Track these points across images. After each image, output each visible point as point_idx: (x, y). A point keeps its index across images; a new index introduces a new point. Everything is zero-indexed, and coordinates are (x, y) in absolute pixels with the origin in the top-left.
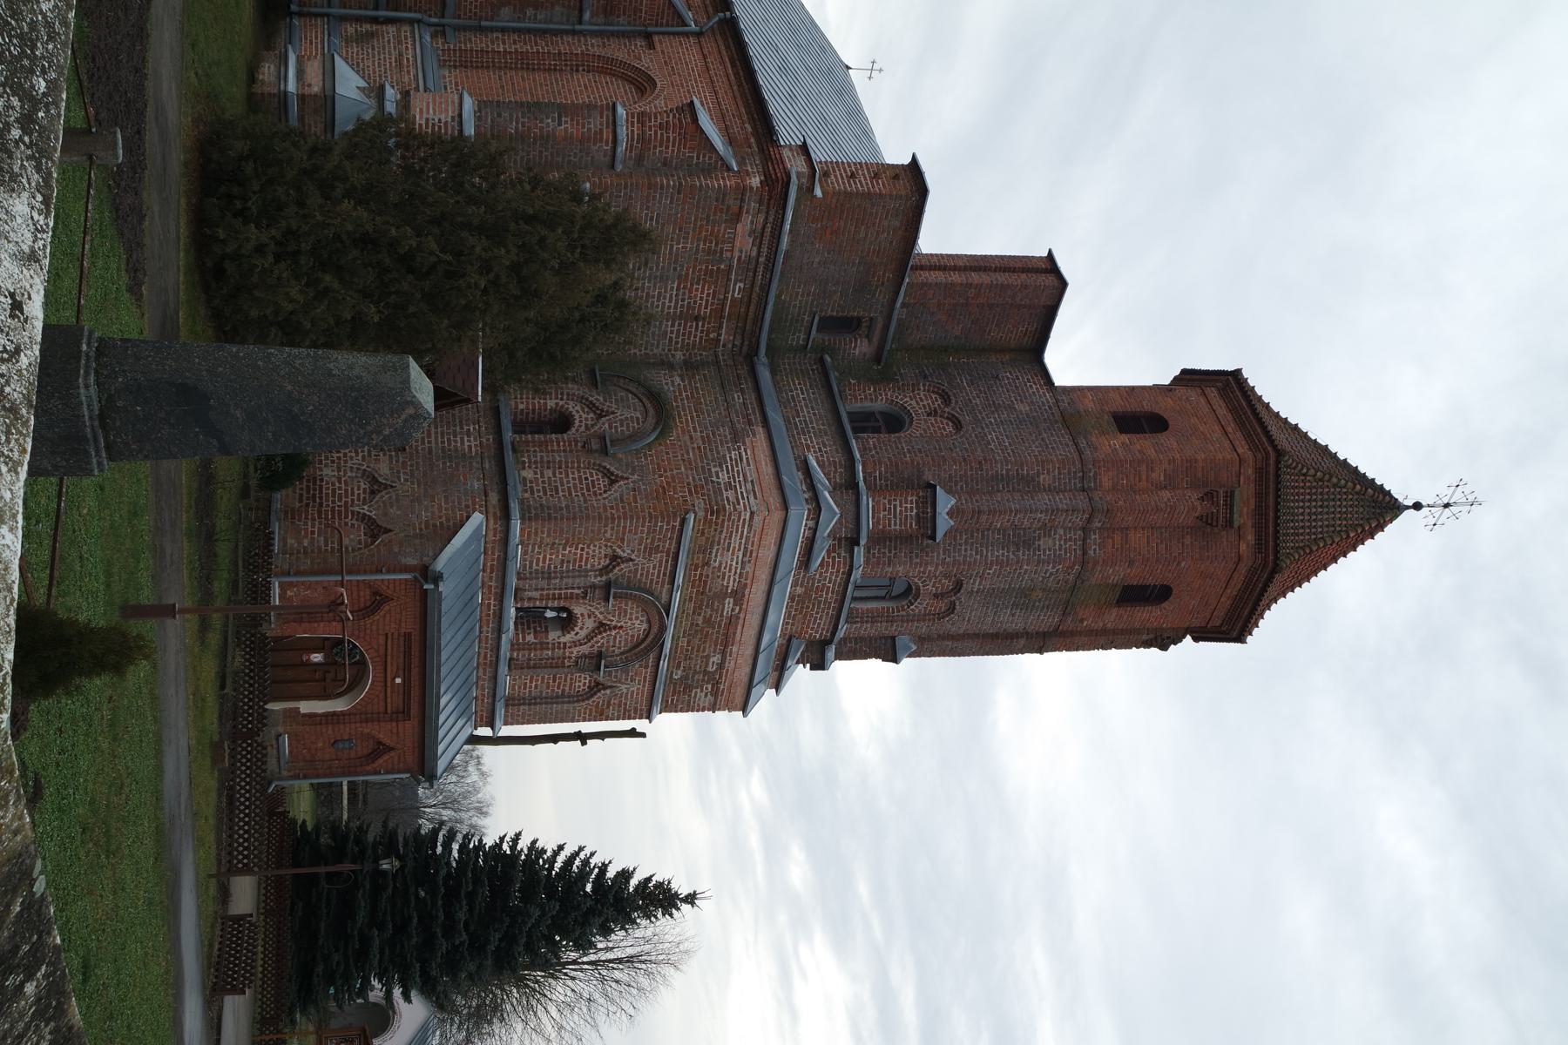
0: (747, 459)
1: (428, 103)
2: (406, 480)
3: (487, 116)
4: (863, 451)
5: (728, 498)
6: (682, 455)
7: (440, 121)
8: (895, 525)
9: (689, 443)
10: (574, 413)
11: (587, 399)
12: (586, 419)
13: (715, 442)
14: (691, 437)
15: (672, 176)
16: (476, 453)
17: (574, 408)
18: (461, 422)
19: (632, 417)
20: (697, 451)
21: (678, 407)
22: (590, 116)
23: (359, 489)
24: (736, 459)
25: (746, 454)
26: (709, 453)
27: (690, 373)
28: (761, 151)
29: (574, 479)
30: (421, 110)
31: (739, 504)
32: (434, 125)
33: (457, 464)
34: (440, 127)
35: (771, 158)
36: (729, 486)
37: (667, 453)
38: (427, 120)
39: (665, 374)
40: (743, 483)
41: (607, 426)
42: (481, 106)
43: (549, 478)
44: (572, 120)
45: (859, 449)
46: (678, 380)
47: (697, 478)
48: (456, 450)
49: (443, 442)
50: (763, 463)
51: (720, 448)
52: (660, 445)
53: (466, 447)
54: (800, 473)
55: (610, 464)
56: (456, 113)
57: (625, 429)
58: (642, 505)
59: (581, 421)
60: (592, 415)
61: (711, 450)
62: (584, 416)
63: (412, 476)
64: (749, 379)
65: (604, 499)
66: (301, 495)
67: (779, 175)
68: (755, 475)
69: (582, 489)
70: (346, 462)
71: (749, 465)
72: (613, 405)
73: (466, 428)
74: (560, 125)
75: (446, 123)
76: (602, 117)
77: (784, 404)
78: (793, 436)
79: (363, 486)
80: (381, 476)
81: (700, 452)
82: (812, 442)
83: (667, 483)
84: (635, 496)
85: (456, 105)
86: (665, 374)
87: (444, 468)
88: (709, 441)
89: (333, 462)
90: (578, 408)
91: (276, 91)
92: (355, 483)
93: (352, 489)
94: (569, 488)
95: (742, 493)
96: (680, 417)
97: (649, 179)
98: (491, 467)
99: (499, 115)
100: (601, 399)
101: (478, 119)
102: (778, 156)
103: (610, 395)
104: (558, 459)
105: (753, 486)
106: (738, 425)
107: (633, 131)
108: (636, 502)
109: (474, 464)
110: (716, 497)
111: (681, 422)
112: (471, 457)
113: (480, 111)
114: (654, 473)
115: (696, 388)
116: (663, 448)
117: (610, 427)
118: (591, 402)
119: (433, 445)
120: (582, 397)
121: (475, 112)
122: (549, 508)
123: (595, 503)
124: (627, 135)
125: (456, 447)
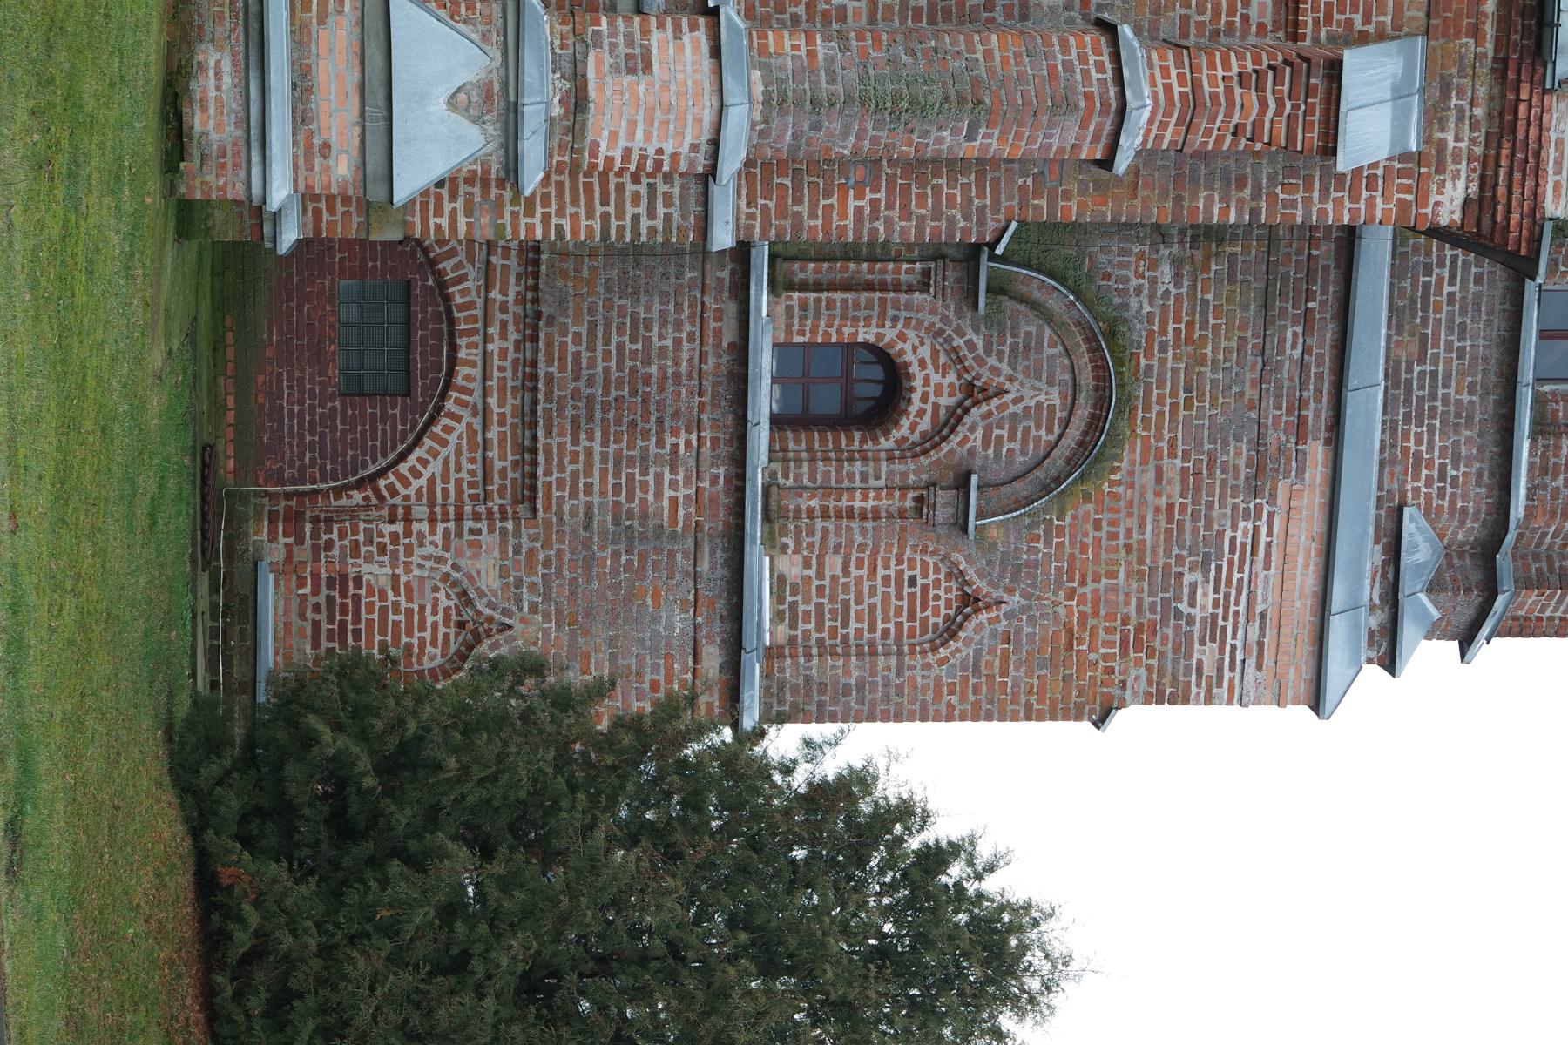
0: (1269, 545)
1: (632, 124)
2: (534, 608)
3: (784, 129)
4: (1542, 470)
5: (1200, 664)
6: (1129, 531)
7: (660, 151)
8: (1556, 609)
9: (1150, 496)
10: (914, 368)
11: (949, 340)
12: (939, 387)
13: (1210, 486)
14: (1159, 471)
15: (1241, 183)
16: (686, 526)
17: (914, 352)
18: (660, 422)
19: (1039, 405)
20: (1163, 518)
21: (1149, 368)
22: (1051, 125)
23: (435, 613)
24: (1243, 545)
25: (1270, 534)
26: (1188, 527)
27: (1199, 255)
28: (1501, 67)
29: (886, 580)
30: (614, 135)
31: (1219, 685)
32: (643, 158)
33: (643, 557)
34: (658, 164)
35: (1514, 131)
36: (1213, 631)
37: (1097, 526)
38: (627, 152)
39: (1141, 256)
40: (1242, 619)
41: (979, 433)
42: (775, 102)
43: (834, 578)
44: (1003, 132)
45: (1531, 466)
46: (1166, 272)
47: (1147, 600)
48: (644, 516)
49: (617, 489)
50: (1301, 559)
51: (1215, 514)
52: (1087, 498)
53: (666, 503)
54: (1379, 548)
55: (969, 560)
56: (706, 136)
57: (1016, 446)
58: (1016, 683)
59: (924, 398)
60: (952, 377)
61: (1195, 516)
62: (935, 378)
63: (547, 597)
64: (1332, 271)
65: (941, 662)
66: (316, 625)
67: (1515, 218)
68: (1273, 597)
69: (899, 611)
70: (409, 550)
71: (1267, 567)
72: (1006, 369)
73: (669, 441)
74: (971, 137)
75: (675, 157)
76: (1084, 125)
77: (1398, 317)
78: (1394, 423)
79: (444, 602)
80: (481, 594)
81: (1170, 520)
82: (1430, 449)
83: (1082, 617)
84: (1005, 656)
85: (708, 116)
86: (1141, 256)
87: (615, 572)
88: (1197, 489)
89: (382, 550)
90: (924, 351)
91: (236, 192)
92: (429, 595)
93: (422, 608)
94: (872, 608)
95: (1234, 648)
96: (1147, 409)
97: (1178, 200)
98: (713, 568)
99: (816, 127)
100: (980, 342)
101: (761, 131)
102: (1533, 131)
103: (1002, 333)
104: (859, 539)
105: (1262, 628)
106: (1272, 437)
107: (1168, 88)
108: (1004, 673)
109: (680, 556)
110: (1175, 662)
111: (1146, 428)
112: (673, 536)
113: (766, 120)
114: (1059, 586)
115: (1205, 303)
116: (1090, 507)
117: (986, 444)
118: (955, 350)
119: (596, 499)
120: (940, 332)
121: (753, 124)
122: (822, 688)
123: (918, 673)
124: (1144, 142)
125: (643, 501)
